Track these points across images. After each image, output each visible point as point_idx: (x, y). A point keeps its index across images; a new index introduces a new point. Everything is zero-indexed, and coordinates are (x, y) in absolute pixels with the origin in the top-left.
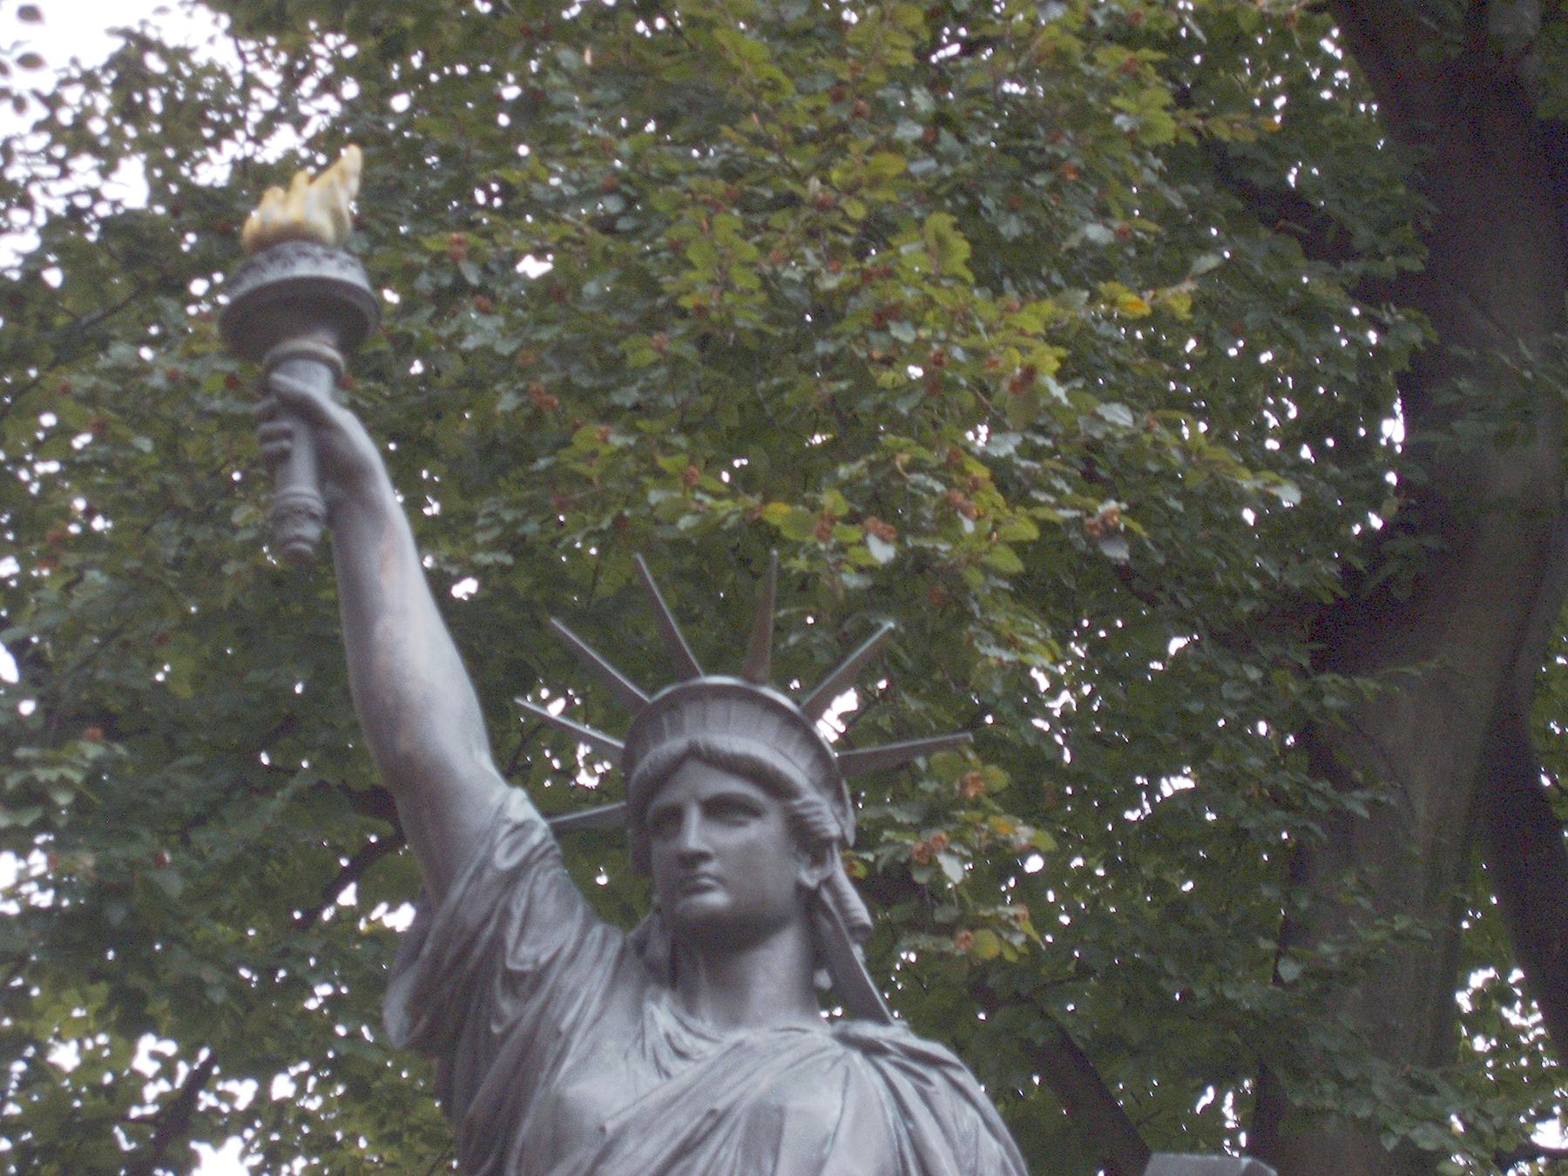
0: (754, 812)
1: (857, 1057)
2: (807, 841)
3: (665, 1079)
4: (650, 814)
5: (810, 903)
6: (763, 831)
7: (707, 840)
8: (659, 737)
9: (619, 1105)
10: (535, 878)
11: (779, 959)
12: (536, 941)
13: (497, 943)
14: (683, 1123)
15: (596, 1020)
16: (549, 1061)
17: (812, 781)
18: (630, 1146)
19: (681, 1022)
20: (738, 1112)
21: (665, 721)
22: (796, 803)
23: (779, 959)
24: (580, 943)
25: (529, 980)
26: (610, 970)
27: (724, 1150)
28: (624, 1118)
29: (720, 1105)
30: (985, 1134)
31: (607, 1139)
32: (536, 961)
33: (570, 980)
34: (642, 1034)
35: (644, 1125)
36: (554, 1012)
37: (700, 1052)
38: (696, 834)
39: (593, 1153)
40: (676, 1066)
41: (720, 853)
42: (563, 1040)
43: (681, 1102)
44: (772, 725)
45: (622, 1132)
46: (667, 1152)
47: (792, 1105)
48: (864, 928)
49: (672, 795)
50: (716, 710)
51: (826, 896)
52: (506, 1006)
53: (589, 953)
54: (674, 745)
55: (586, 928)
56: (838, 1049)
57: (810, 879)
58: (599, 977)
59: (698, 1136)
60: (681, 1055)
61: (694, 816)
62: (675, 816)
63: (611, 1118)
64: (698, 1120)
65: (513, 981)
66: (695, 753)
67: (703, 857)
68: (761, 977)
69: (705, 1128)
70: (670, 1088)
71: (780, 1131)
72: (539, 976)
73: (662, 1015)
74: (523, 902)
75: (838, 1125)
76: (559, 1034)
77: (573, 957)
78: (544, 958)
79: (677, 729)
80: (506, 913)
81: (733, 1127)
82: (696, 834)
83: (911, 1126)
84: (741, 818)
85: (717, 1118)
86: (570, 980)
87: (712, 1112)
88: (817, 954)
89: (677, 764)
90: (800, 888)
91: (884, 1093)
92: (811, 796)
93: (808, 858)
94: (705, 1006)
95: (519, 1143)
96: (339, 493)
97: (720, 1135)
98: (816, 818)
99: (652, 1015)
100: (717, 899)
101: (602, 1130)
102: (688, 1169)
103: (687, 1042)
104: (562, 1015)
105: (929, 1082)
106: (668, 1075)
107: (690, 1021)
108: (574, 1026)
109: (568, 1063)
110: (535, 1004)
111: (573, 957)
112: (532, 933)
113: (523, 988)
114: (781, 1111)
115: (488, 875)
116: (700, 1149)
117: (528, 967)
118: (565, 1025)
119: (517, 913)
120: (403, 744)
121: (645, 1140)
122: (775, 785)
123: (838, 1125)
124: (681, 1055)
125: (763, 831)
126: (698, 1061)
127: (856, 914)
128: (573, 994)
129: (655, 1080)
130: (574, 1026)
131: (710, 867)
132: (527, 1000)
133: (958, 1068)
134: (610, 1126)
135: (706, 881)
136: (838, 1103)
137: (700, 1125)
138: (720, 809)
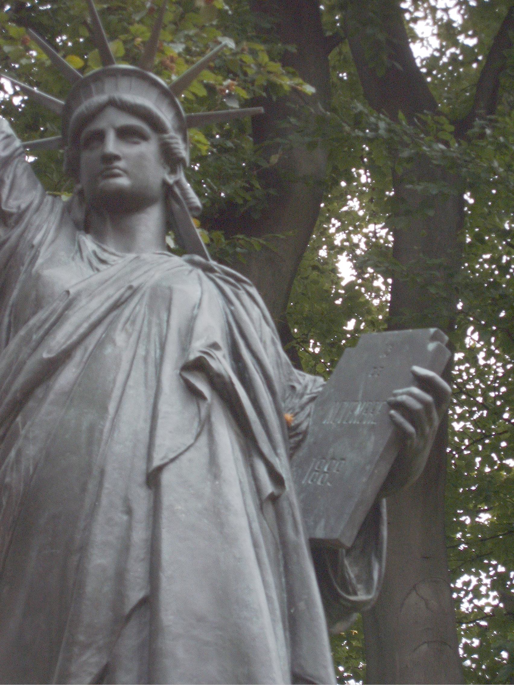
0: (144, 137)
1: (200, 272)
3: (96, 272)
4: (83, 135)
5: (168, 192)
6: (149, 149)
8: (89, 95)
9: (74, 282)
10: (17, 164)
11: (150, 220)
12: (16, 199)
14: (114, 293)
15: (53, 241)
16: (27, 260)
17: (173, 127)
18: (83, 301)
19: (100, 247)
20: (144, 289)
21: (93, 87)
22: (166, 136)
23: (150, 220)
24: (41, 203)
26: (59, 217)
27: (137, 307)
28: (79, 287)
29: (135, 284)
30: (263, 322)
31: (70, 297)
32: (19, 207)
33: (37, 220)
34: (80, 250)
37: (114, 261)
38: (112, 145)
39: (62, 305)
40: (102, 267)
41: (126, 157)
42: (35, 250)
43: (109, 282)
44: (154, 94)
45: (78, 294)
46: (103, 309)
47: (177, 286)
48: (197, 208)
49: (101, 124)
50: (124, 82)
51: (177, 190)
53: (47, 208)
54: (102, 98)
55: (43, 196)
56: (189, 267)
59: (122, 300)
60: (103, 262)
62: (100, 136)
63: (72, 286)
64: (122, 290)
66: (113, 103)
67: (117, 158)
69: (127, 295)
70: (98, 277)
71: (170, 300)
72: (21, 215)
73: (89, 243)
74: (11, 176)
75: (201, 300)
76: (33, 246)
77: (38, 209)
78: (23, 206)
79: (101, 91)
81: (143, 295)
82: (112, 145)
83: (232, 308)
84: (136, 140)
85: (133, 291)
86: (37, 220)
87: (130, 287)
88: (170, 224)
89: (101, 108)
90: (165, 183)
92: (172, 133)
93: (168, 169)
95: (10, 303)
97: (136, 299)
98: (176, 146)
99: (84, 242)
100: (123, 181)
101: (68, 292)
102: (118, 317)
104: (33, 237)
105: (239, 289)
106: (98, 270)
107: (105, 247)
108: (41, 244)
109: (40, 261)
110: (18, 231)
111: (38, 209)
112: (15, 193)
113: (11, 221)
114: (170, 289)
116: (123, 306)
117: (14, 210)
118: (36, 241)
119: (8, 182)
121: (91, 300)
122: (157, 126)
123: (201, 300)
124: (103, 262)
125: (149, 149)
126: (112, 265)
127: (193, 200)
128: (39, 228)
129: (91, 272)
130: (41, 244)
131: (121, 164)
132: (13, 228)
133: (250, 285)
134: (72, 291)
135: (117, 171)
136: (199, 289)
137: (122, 296)
138: (126, 134)
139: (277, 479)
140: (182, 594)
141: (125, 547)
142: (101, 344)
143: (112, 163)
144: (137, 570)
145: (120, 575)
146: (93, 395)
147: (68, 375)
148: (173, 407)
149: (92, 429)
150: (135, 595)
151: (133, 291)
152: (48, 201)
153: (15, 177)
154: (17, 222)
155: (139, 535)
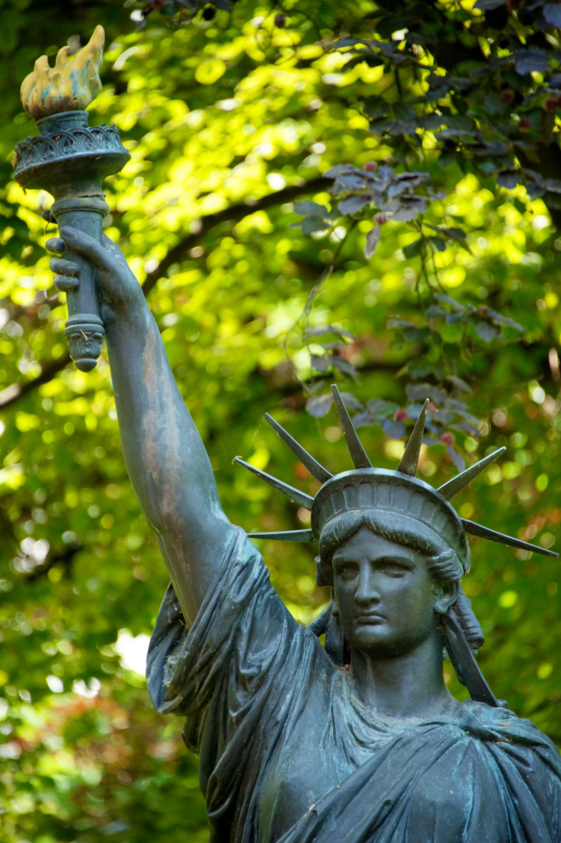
1: (478, 744)
7: (376, 588)
12: (258, 650)
13: (233, 650)
15: (301, 712)
22: (435, 558)
25: (255, 681)
29: (391, 797)
33: (282, 679)
36: (271, 703)
51: (453, 616)
52: (240, 696)
56: (467, 740)
57: (442, 604)
58: (302, 674)
61: (366, 571)
65: (243, 681)
67: (375, 601)
68: (409, 677)
78: (265, 665)
79: (354, 504)
80: (238, 630)
89: (354, 531)
91: (497, 775)
96: (112, 314)
97: (393, 820)
103: (364, 732)
113: (251, 686)
115: (226, 606)
116: (380, 830)
119: (245, 630)
128: (285, 690)
143: (368, 608)
152: (296, 643)
153: (254, 620)
154: (258, 687)
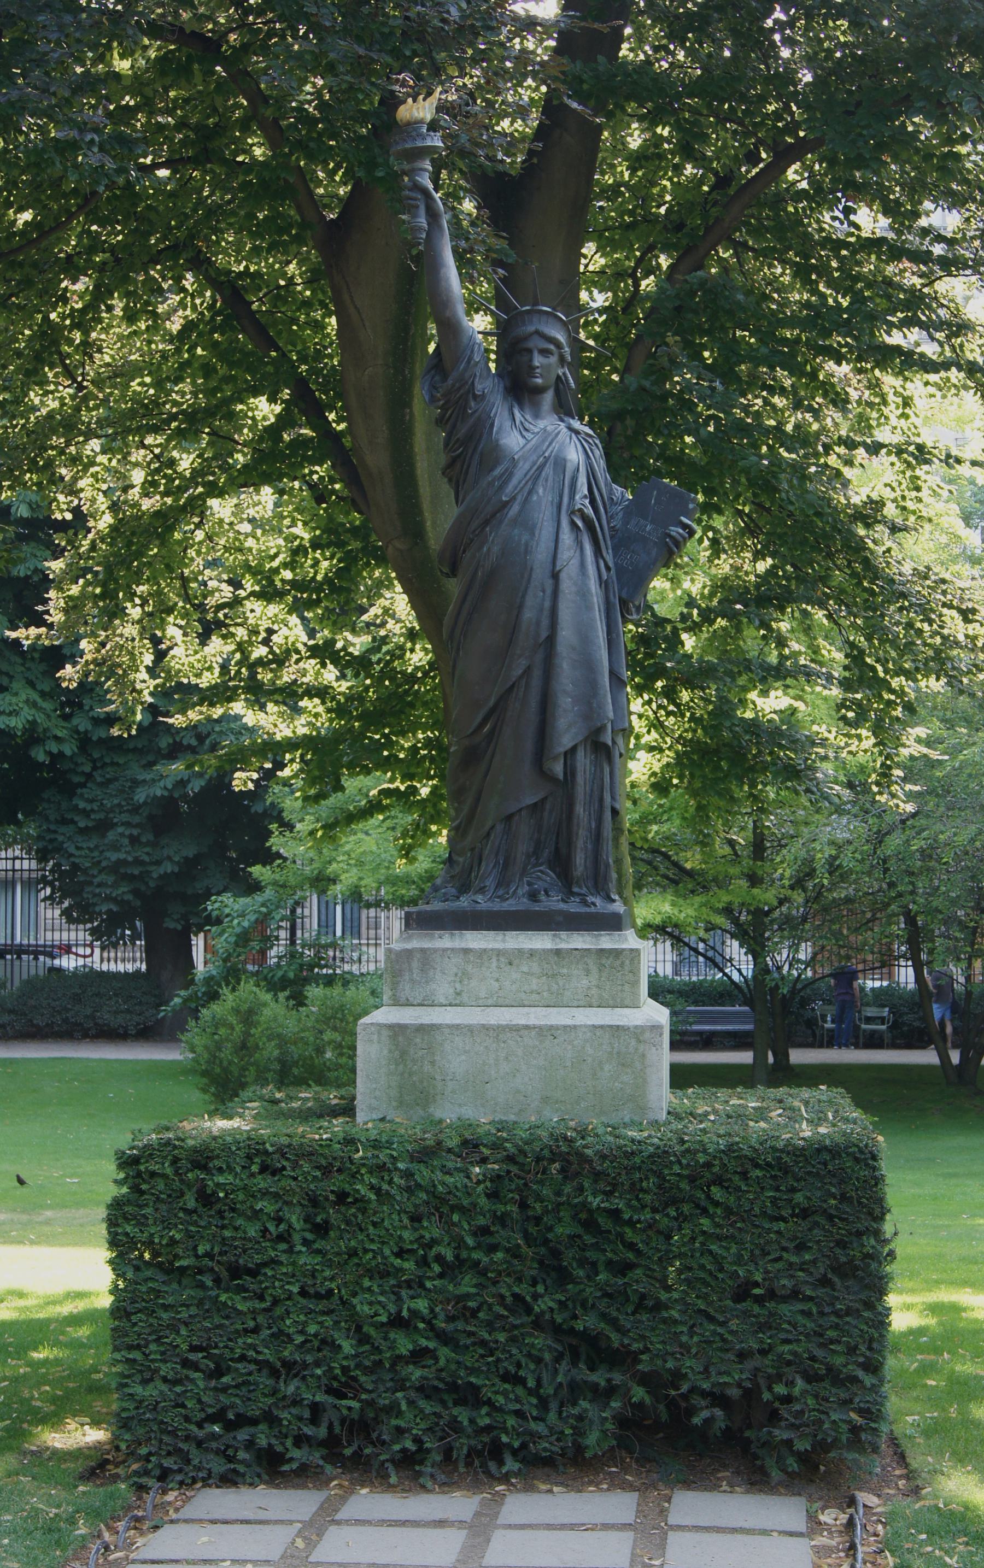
2: (562, 360)
27: (548, 470)
35: (525, 458)
49: (530, 344)
54: (531, 329)
57: (560, 372)
61: (536, 354)
65: (475, 397)
66: (537, 332)
85: (547, 459)
89: (531, 335)
94: (527, 410)
100: (539, 381)
120: (448, 314)
125: (553, 359)
138: (545, 352)
139: (608, 568)
140: (566, 635)
141: (541, 610)
142: (530, 492)
144: (545, 622)
145: (538, 623)
146: (526, 523)
147: (515, 508)
148: (567, 536)
149: (527, 545)
150: (544, 634)
151: (547, 459)
155: (547, 604)
